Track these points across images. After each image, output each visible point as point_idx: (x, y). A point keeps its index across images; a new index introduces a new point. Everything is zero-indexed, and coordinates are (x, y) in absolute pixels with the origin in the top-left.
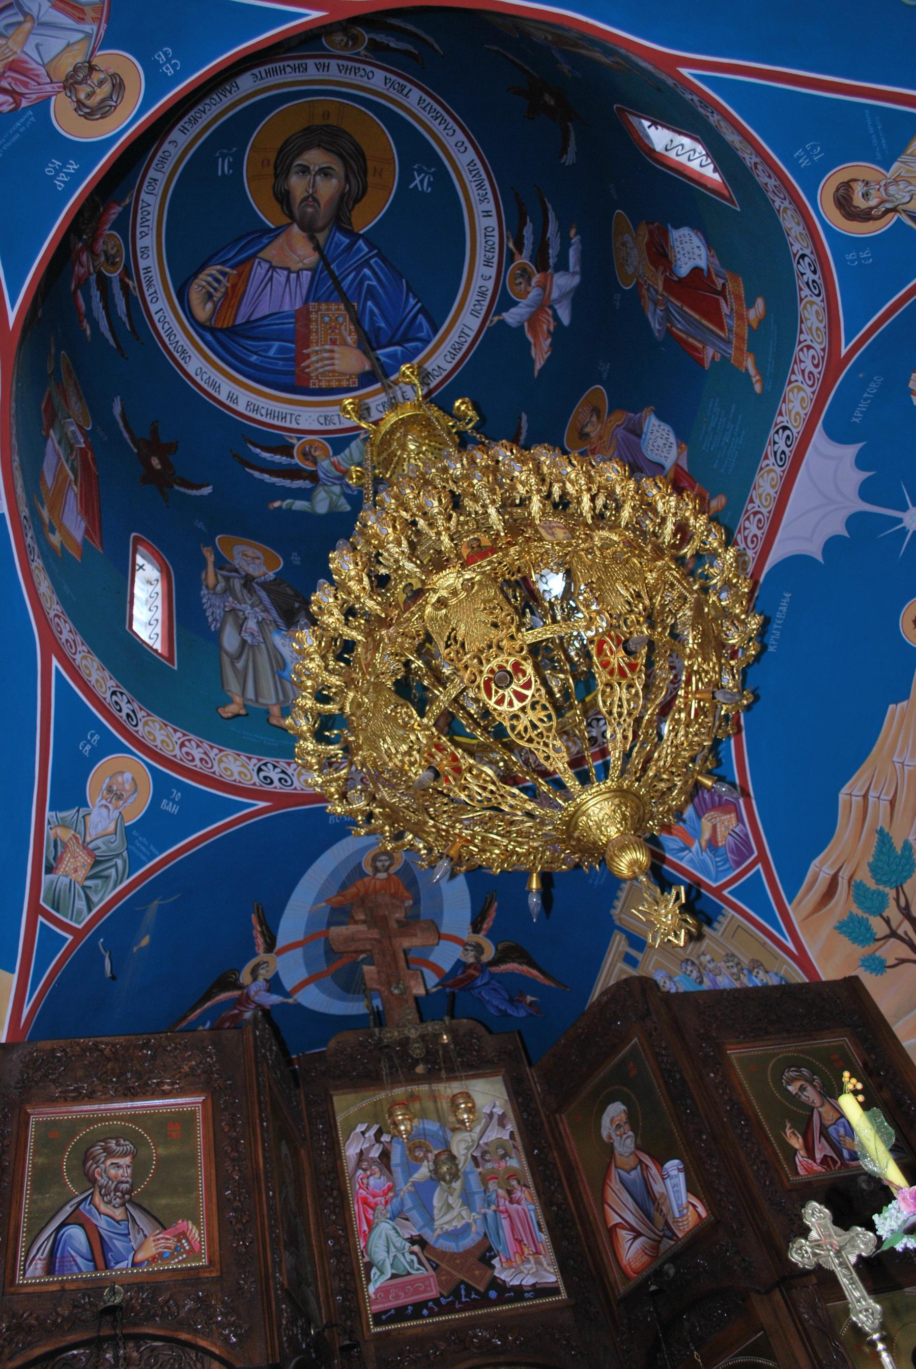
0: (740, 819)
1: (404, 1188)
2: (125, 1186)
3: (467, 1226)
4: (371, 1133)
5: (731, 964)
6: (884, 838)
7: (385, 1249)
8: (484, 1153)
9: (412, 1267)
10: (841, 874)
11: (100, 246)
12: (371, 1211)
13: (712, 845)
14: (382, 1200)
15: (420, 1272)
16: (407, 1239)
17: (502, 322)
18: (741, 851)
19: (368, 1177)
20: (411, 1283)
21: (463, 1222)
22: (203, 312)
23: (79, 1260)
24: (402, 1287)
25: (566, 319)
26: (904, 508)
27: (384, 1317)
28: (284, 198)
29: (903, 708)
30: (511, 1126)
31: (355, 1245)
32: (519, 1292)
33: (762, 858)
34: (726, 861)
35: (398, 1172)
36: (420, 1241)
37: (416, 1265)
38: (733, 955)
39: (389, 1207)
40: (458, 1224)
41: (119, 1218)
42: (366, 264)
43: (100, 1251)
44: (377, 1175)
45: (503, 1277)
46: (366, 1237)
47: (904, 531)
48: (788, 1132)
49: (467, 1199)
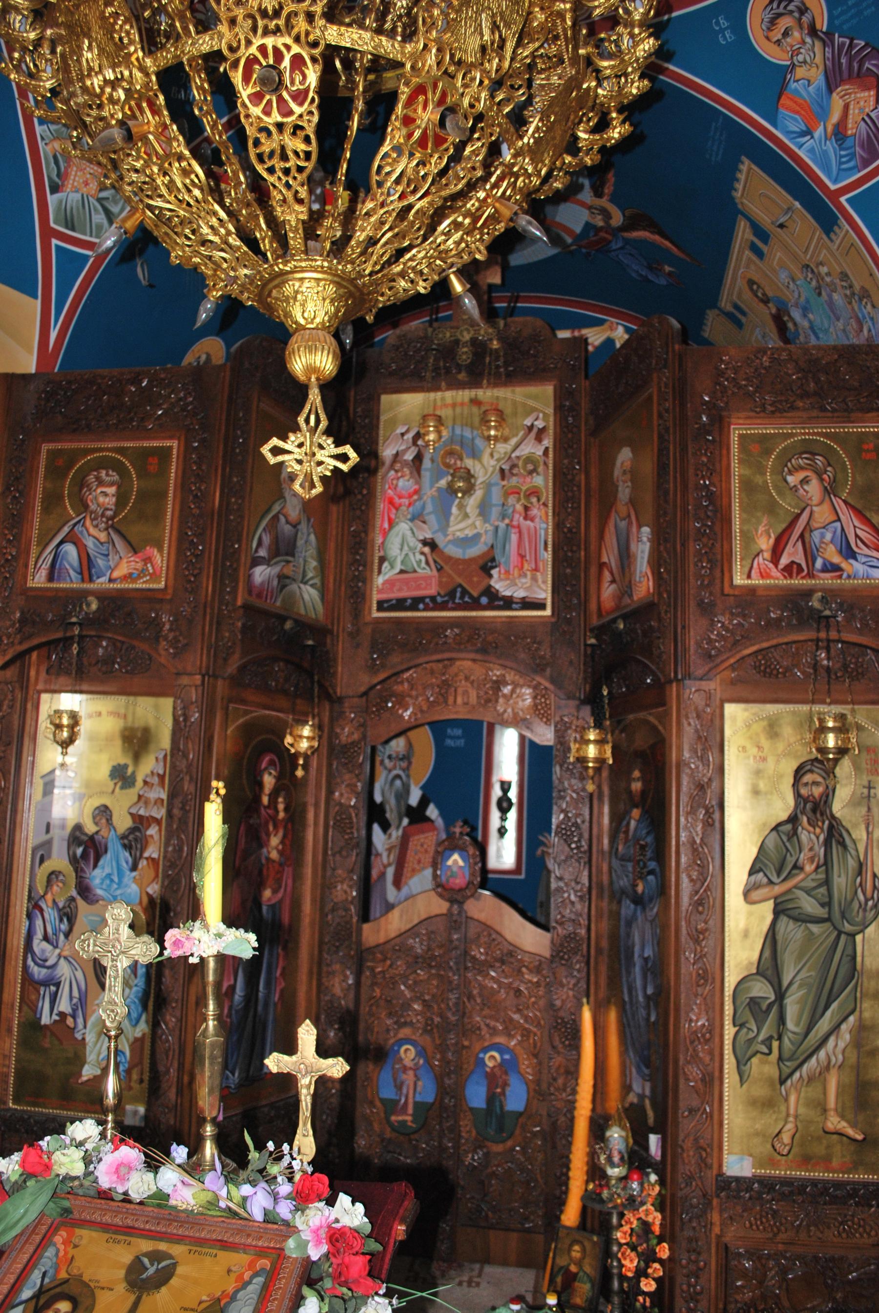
1: (429, 492)
2: (109, 513)
3: (477, 536)
4: (410, 436)
5: (844, 284)
8: (513, 466)
9: (419, 566)
12: (394, 511)
13: (839, 133)
14: (406, 501)
15: (425, 571)
16: (421, 541)
19: (398, 479)
20: (416, 580)
21: (475, 531)
23: (72, 572)
24: (406, 582)
27: (386, 605)
30: (548, 442)
31: (373, 540)
32: (508, 603)
34: (852, 156)
35: (426, 475)
36: (431, 544)
37: (423, 565)
38: (846, 275)
39: (411, 509)
40: (470, 533)
41: (103, 540)
43: (87, 568)
44: (407, 478)
45: (497, 587)
46: (385, 534)
48: (761, 529)
49: (484, 509)
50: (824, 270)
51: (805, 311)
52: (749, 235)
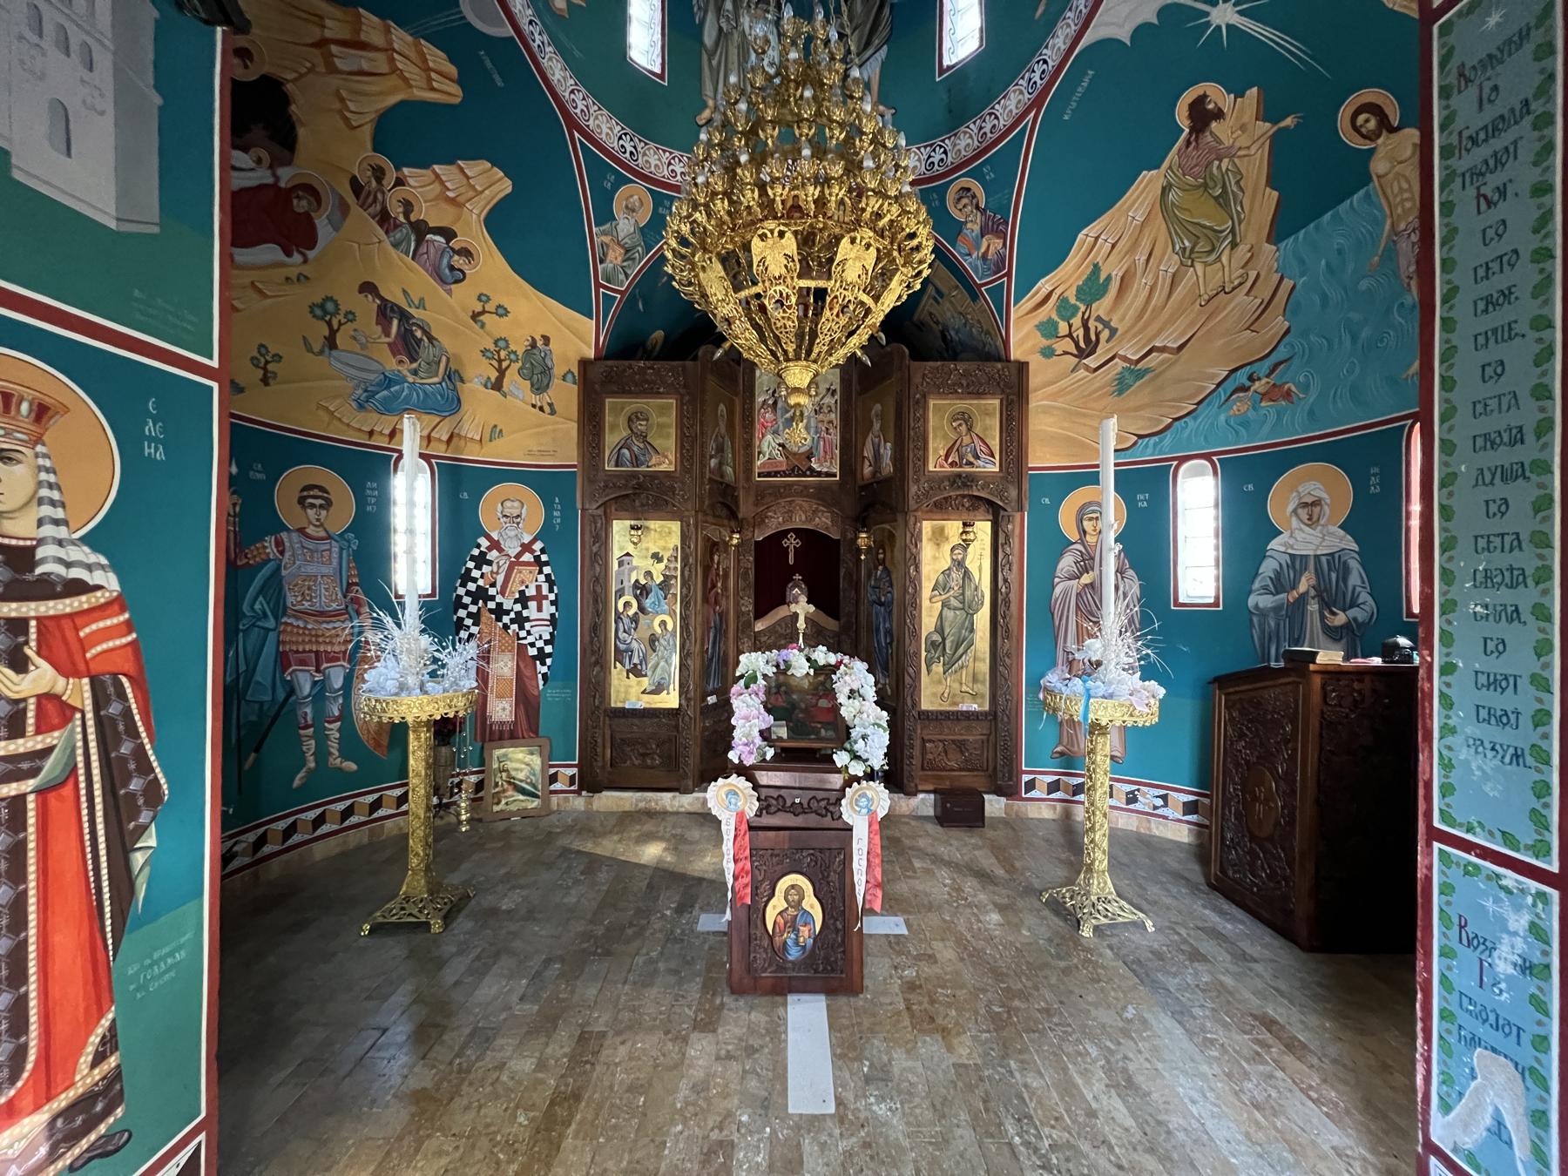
7: (768, 447)
13: (984, 257)
30: (837, 397)
32: (819, 474)
47: (1208, 24)
49: (807, 428)
51: (957, 332)
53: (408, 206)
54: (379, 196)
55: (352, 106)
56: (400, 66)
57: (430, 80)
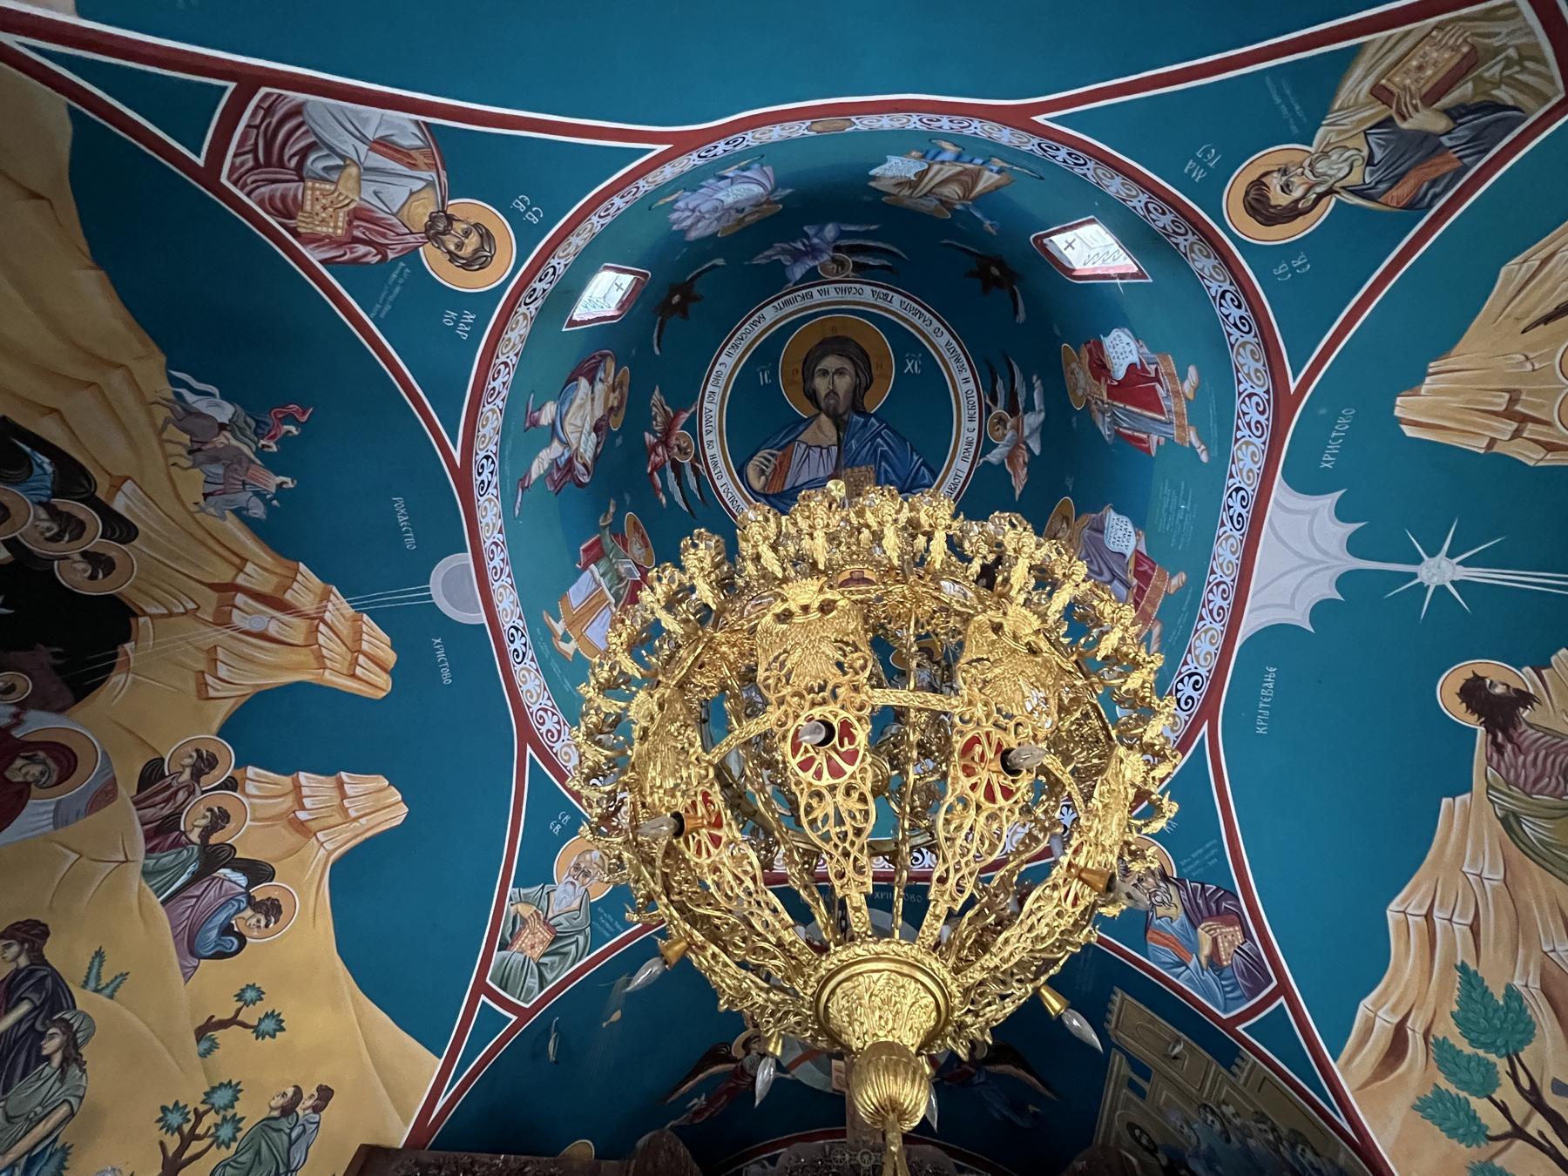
0: (1247, 934)
5: (1263, 1126)
6: (1470, 980)
10: (1409, 1024)
11: (673, 441)
13: (1214, 961)
17: (987, 463)
18: (1254, 974)
22: (758, 484)
25: (1037, 452)
26: (1419, 560)
28: (812, 396)
29: (1464, 803)
33: (1283, 988)
34: (1236, 986)
38: (1263, 1115)
42: (879, 434)
47: (1422, 588)
50: (1229, 1110)
52: (1126, 1070)
53: (220, 819)
54: (181, 796)
55: (223, 671)
56: (321, 639)
57: (355, 662)
